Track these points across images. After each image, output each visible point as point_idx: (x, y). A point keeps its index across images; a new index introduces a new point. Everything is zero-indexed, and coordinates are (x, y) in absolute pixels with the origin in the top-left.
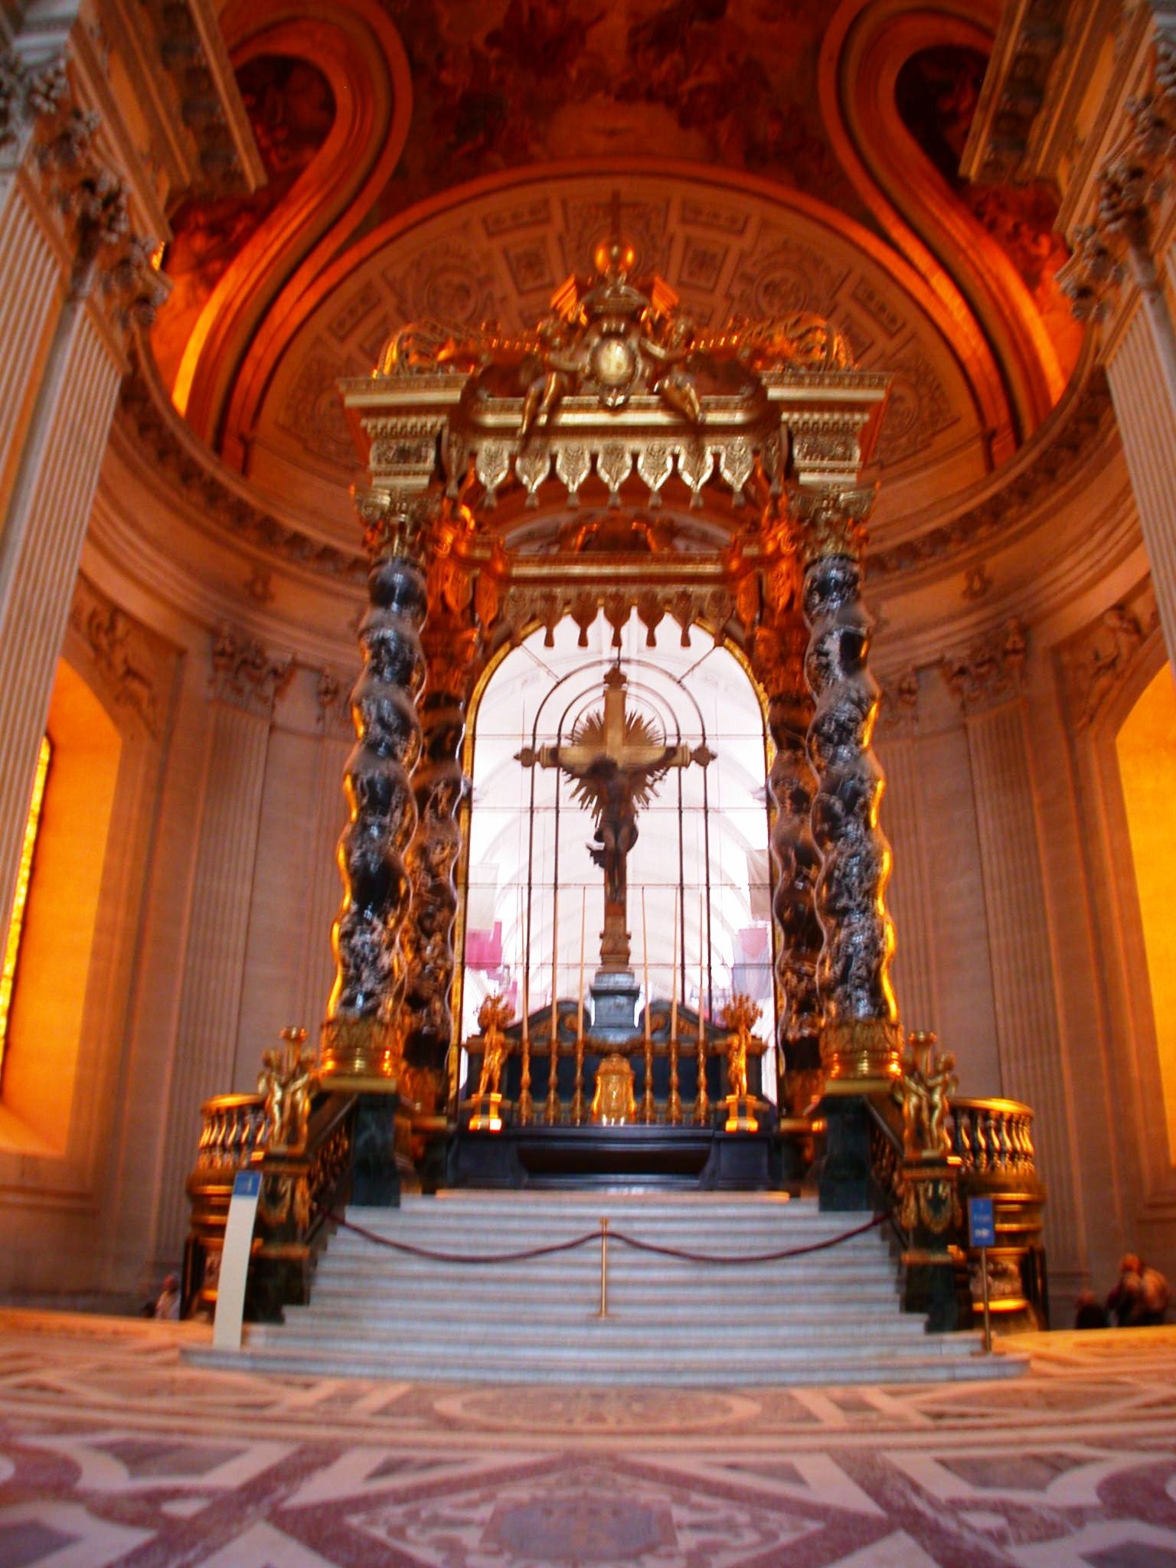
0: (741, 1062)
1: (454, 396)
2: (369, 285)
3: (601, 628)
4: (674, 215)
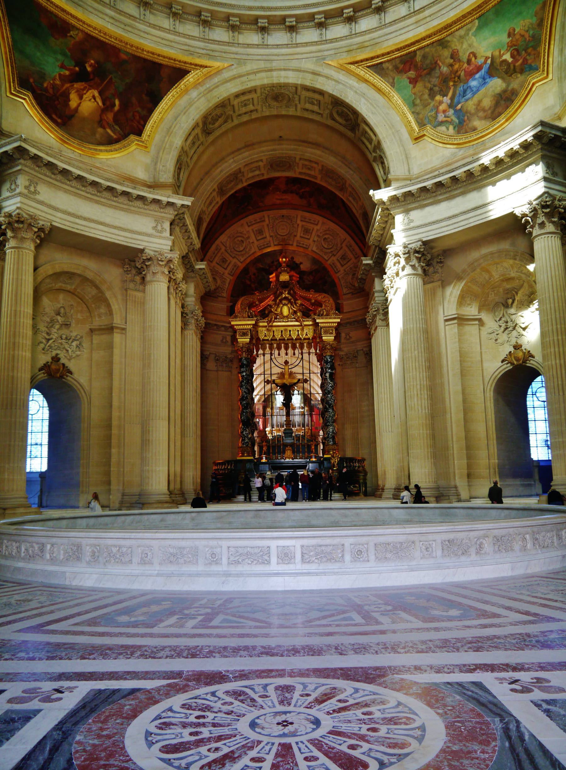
0: (313, 447)
1: (254, 322)
2: (218, 245)
3: (283, 351)
4: (299, 219)
